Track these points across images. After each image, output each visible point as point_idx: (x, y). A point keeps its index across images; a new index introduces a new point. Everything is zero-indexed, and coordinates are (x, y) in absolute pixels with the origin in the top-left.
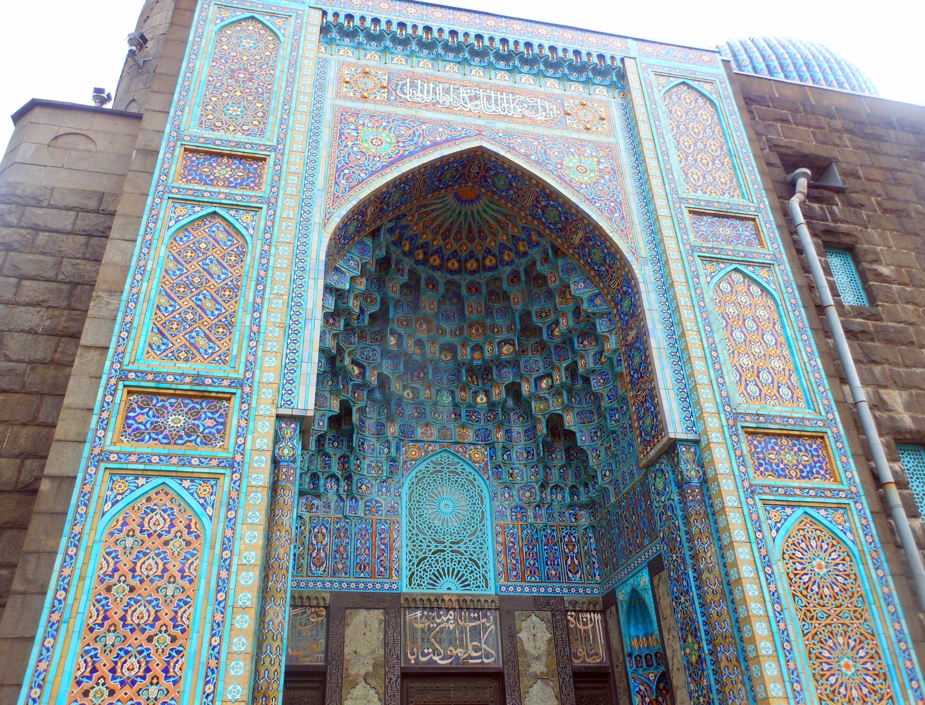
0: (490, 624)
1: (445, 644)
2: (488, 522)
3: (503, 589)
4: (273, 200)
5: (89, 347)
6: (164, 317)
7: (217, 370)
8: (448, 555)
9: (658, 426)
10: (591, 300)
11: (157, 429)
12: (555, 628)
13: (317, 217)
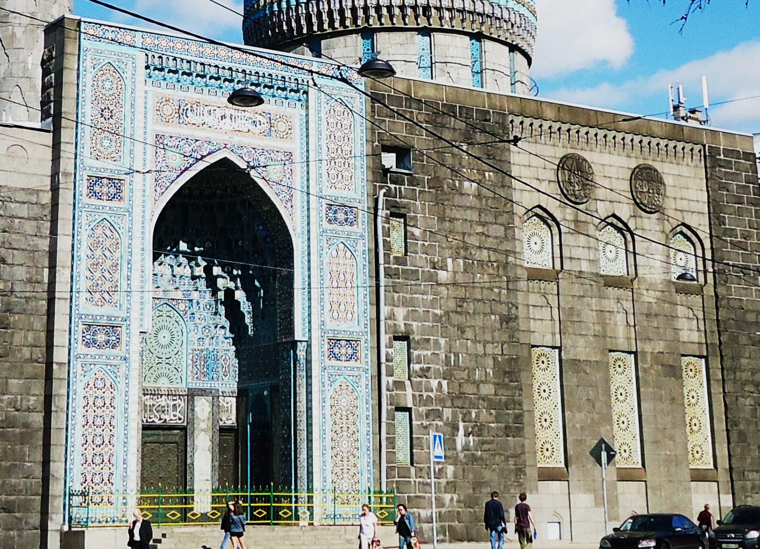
0: (182, 403)
1: (160, 413)
2: (184, 346)
3: (190, 384)
4: (131, 210)
5: (59, 299)
6: (90, 283)
7: (115, 312)
8: (164, 365)
9: (292, 332)
10: (265, 239)
11: (95, 342)
12: (213, 405)
13: (148, 216)
